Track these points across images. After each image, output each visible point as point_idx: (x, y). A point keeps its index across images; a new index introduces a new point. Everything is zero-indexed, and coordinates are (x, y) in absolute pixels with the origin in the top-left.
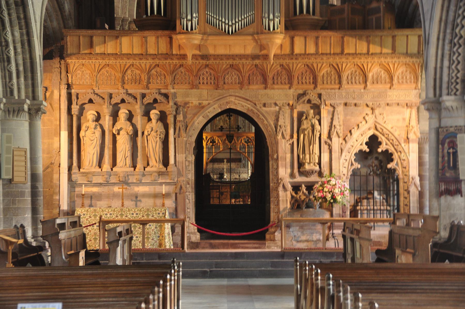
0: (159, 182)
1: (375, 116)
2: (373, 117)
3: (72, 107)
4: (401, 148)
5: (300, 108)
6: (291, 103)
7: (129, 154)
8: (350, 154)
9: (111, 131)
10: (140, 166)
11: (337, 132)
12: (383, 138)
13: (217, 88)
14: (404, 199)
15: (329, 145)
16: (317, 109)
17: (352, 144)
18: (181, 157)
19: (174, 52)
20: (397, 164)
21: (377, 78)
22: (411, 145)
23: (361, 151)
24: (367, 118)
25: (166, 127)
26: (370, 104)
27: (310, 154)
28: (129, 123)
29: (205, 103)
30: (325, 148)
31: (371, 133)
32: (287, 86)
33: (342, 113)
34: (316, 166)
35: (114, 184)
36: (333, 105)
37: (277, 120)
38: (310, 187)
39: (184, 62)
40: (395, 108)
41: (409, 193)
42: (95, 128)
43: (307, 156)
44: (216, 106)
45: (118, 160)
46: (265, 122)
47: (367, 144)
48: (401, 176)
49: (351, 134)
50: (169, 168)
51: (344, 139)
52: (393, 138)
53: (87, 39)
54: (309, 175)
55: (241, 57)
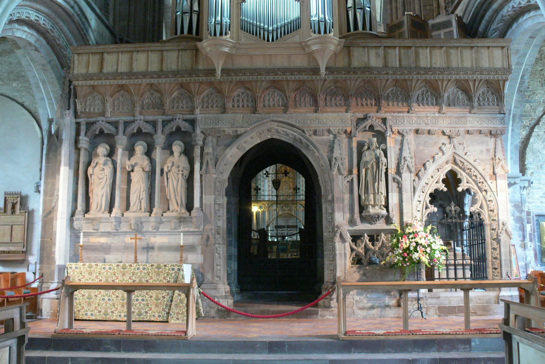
0: (180, 230)
1: (454, 146)
2: (451, 147)
3: (81, 138)
4: (487, 186)
5: (360, 136)
6: (349, 130)
7: (144, 195)
8: (425, 194)
9: (123, 168)
11: (408, 166)
13: (255, 111)
14: (492, 250)
15: (398, 183)
16: (382, 137)
17: (427, 181)
18: (209, 199)
19: (201, 67)
20: (481, 207)
21: (454, 100)
23: (436, 190)
24: (444, 148)
26: (447, 131)
27: (374, 194)
28: (146, 158)
29: (240, 130)
30: (393, 186)
31: (448, 168)
32: (343, 109)
33: (413, 142)
34: (383, 209)
35: (125, 233)
36: (401, 132)
37: (332, 150)
38: (373, 238)
39: (213, 79)
40: (477, 137)
41: (499, 242)
42: (105, 164)
43: (371, 197)
44: (253, 134)
45: (132, 203)
46: (317, 154)
47: (444, 181)
48: (487, 221)
49: (425, 169)
50: (194, 213)
51: (417, 175)
52: (476, 173)
53: (97, 57)
54: (374, 222)
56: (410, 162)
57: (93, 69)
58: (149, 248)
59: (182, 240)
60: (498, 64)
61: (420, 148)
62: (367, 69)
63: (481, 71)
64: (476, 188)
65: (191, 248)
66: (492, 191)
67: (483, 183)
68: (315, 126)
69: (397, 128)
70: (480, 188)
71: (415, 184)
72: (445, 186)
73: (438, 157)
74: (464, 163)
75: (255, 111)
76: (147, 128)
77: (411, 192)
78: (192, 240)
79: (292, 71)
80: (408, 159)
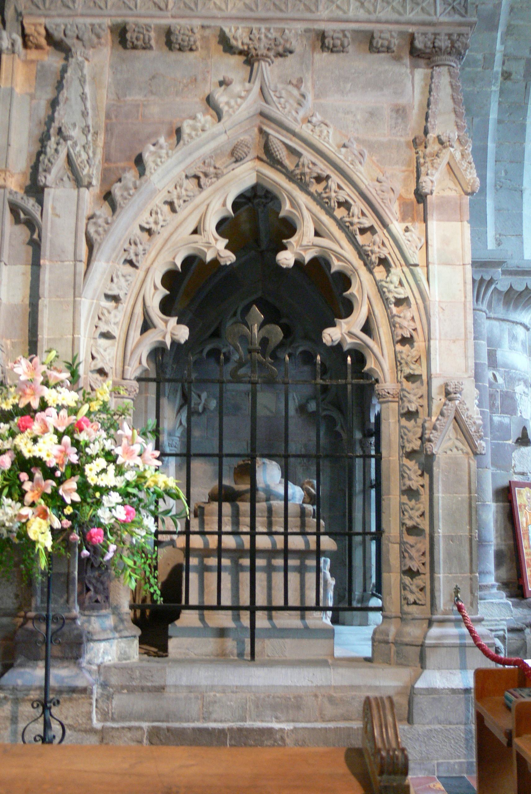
1: (261, 89)
2: (248, 91)
4: (389, 243)
8: (141, 273)
12: (302, 198)
14: (405, 499)
17: (145, 219)
20: (367, 329)
22: (433, 224)
33: (107, 77)
36: (58, 35)
61: (129, 98)
64: (349, 253)
66: (408, 264)
67: (371, 229)
69: (42, 20)
70: (363, 254)
71: (92, 230)
72: (227, 247)
73: (194, 128)
74: (299, 155)
77: (76, 260)
80: (75, 133)
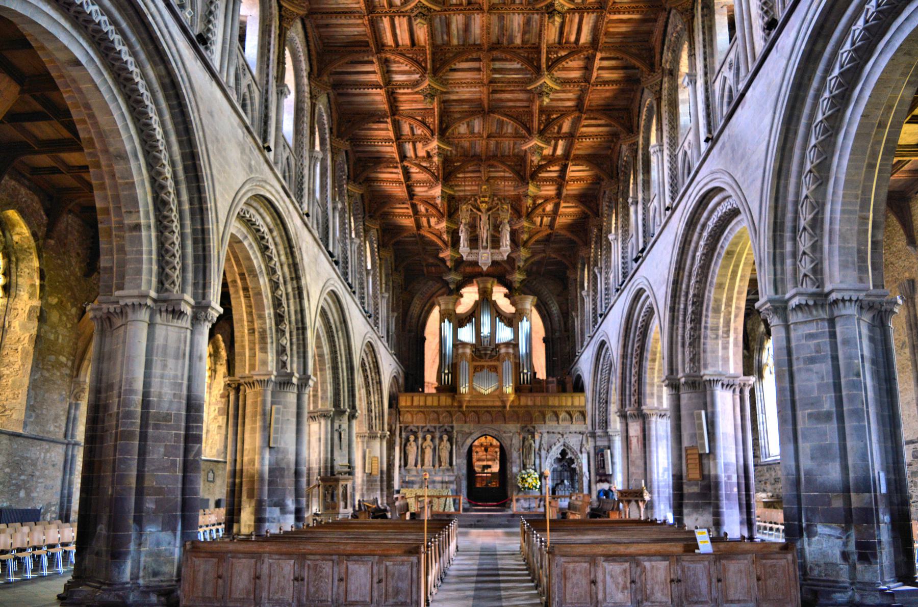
10: (437, 465)
13: (479, 422)
25: (452, 445)
31: (562, 448)
55: (491, 407)
56: (545, 446)
57: (409, 404)
58: (434, 482)
59: (447, 479)
60: (583, 404)
62: (527, 406)
63: (575, 407)
65: (450, 482)
68: (505, 429)
75: (479, 422)
76: (432, 429)
78: (452, 478)
79: (494, 407)
